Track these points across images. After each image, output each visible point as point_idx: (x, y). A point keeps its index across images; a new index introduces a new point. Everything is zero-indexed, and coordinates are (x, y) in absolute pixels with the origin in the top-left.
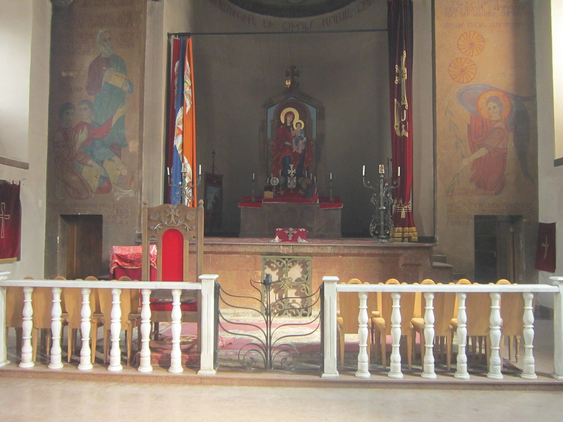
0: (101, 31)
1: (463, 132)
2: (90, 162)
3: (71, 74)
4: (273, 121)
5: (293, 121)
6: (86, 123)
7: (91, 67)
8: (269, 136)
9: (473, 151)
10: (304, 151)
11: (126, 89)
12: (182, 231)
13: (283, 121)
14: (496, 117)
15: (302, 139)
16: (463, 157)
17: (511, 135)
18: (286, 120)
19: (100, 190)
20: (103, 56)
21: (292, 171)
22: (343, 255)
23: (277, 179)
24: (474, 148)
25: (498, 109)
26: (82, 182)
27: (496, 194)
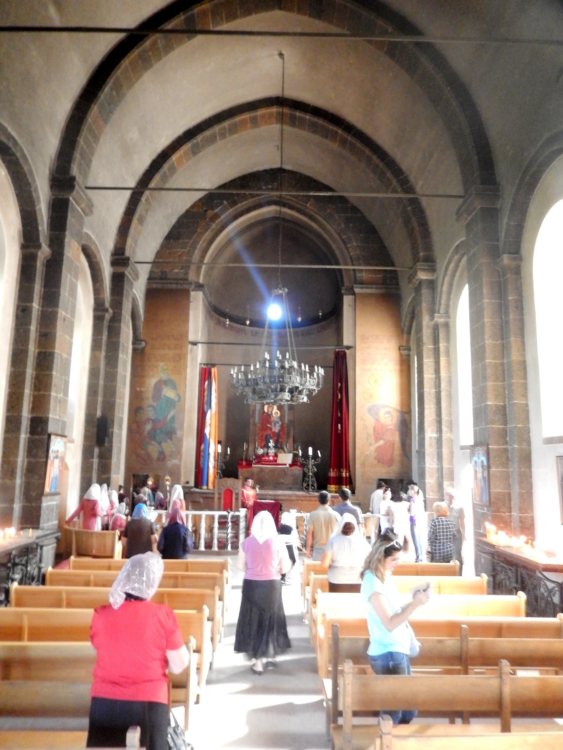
0: (162, 364)
1: (371, 431)
2: (153, 442)
3: (143, 389)
4: (260, 410)
5: (272, 411)
6: (152, 420)
7: (156, 385)
8: (257, 420)
9: (376, 442)
10: (280, 431)
11: (176, 399)
12: (232, 490)
13: (266, 411)
14: (389, 422)
15: (278, 423)
16: (371, 445)
17: (397, 433)
18: (268, 410)
19: (159, 459)
20: (163, 379)
21: (271, 444)
22: (302, 500)
23: (262, 450)
24: (377, 439)
25: (390, 418)
26: (148, 455)
27: (389, 466)
